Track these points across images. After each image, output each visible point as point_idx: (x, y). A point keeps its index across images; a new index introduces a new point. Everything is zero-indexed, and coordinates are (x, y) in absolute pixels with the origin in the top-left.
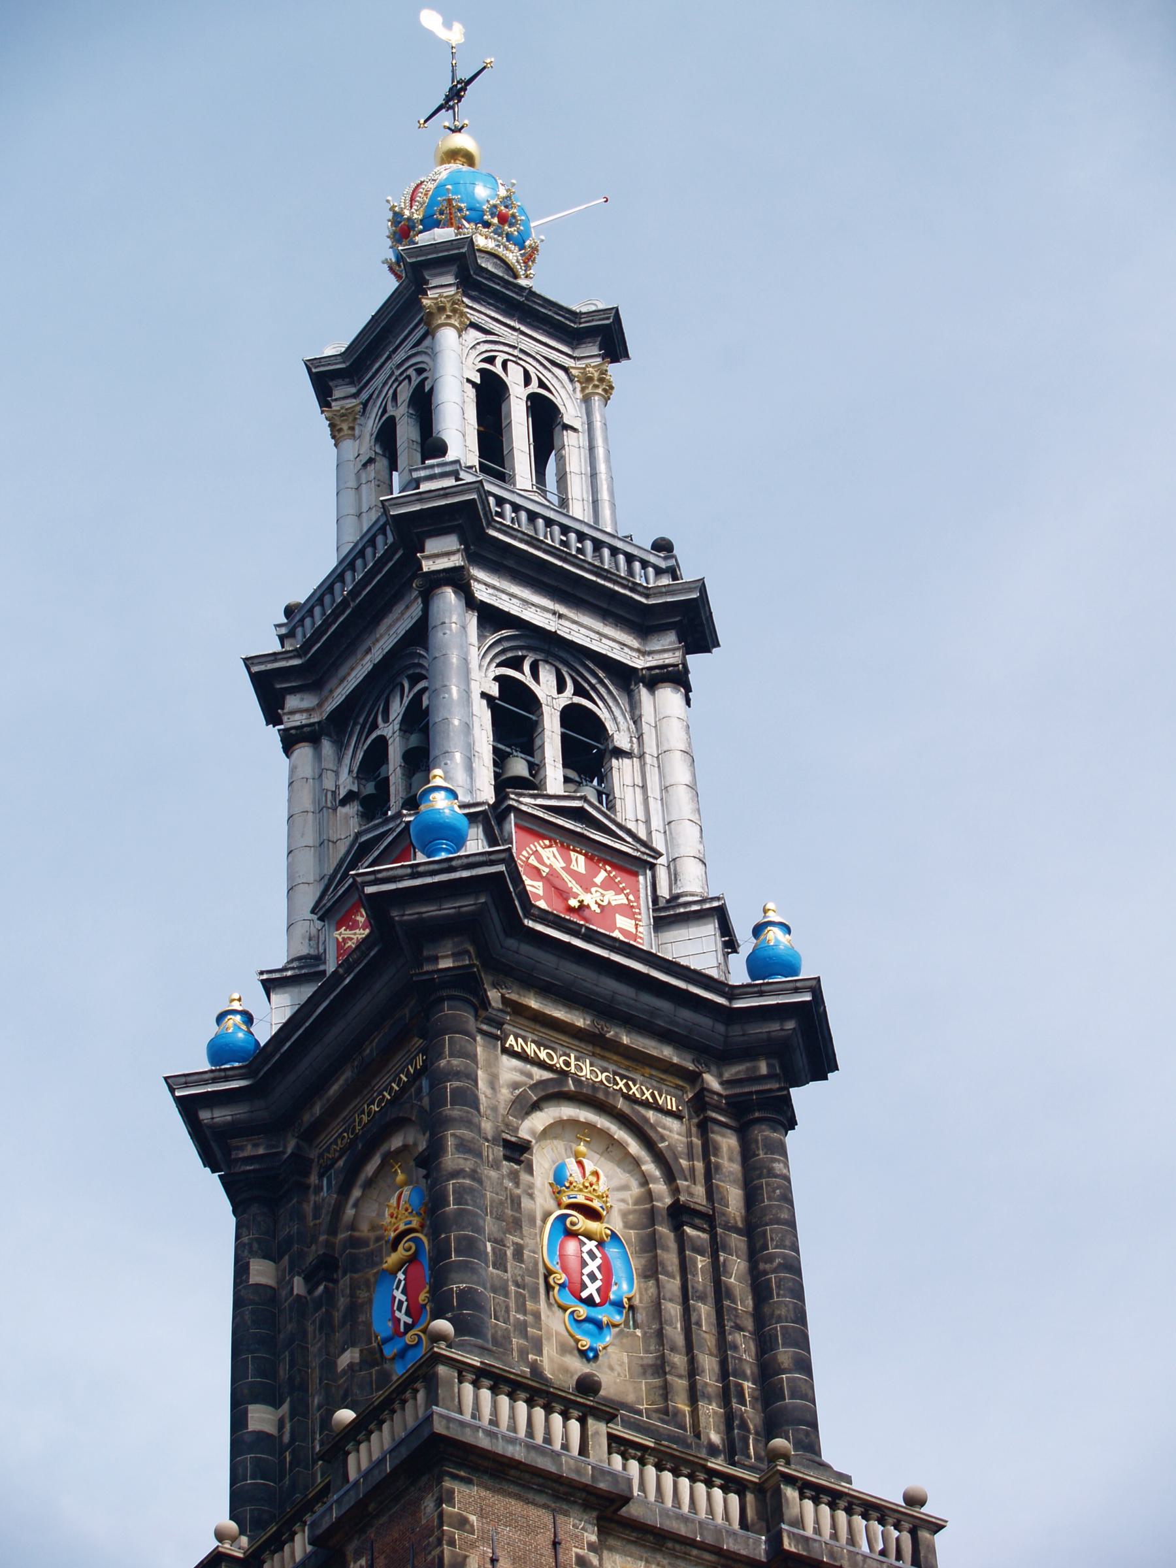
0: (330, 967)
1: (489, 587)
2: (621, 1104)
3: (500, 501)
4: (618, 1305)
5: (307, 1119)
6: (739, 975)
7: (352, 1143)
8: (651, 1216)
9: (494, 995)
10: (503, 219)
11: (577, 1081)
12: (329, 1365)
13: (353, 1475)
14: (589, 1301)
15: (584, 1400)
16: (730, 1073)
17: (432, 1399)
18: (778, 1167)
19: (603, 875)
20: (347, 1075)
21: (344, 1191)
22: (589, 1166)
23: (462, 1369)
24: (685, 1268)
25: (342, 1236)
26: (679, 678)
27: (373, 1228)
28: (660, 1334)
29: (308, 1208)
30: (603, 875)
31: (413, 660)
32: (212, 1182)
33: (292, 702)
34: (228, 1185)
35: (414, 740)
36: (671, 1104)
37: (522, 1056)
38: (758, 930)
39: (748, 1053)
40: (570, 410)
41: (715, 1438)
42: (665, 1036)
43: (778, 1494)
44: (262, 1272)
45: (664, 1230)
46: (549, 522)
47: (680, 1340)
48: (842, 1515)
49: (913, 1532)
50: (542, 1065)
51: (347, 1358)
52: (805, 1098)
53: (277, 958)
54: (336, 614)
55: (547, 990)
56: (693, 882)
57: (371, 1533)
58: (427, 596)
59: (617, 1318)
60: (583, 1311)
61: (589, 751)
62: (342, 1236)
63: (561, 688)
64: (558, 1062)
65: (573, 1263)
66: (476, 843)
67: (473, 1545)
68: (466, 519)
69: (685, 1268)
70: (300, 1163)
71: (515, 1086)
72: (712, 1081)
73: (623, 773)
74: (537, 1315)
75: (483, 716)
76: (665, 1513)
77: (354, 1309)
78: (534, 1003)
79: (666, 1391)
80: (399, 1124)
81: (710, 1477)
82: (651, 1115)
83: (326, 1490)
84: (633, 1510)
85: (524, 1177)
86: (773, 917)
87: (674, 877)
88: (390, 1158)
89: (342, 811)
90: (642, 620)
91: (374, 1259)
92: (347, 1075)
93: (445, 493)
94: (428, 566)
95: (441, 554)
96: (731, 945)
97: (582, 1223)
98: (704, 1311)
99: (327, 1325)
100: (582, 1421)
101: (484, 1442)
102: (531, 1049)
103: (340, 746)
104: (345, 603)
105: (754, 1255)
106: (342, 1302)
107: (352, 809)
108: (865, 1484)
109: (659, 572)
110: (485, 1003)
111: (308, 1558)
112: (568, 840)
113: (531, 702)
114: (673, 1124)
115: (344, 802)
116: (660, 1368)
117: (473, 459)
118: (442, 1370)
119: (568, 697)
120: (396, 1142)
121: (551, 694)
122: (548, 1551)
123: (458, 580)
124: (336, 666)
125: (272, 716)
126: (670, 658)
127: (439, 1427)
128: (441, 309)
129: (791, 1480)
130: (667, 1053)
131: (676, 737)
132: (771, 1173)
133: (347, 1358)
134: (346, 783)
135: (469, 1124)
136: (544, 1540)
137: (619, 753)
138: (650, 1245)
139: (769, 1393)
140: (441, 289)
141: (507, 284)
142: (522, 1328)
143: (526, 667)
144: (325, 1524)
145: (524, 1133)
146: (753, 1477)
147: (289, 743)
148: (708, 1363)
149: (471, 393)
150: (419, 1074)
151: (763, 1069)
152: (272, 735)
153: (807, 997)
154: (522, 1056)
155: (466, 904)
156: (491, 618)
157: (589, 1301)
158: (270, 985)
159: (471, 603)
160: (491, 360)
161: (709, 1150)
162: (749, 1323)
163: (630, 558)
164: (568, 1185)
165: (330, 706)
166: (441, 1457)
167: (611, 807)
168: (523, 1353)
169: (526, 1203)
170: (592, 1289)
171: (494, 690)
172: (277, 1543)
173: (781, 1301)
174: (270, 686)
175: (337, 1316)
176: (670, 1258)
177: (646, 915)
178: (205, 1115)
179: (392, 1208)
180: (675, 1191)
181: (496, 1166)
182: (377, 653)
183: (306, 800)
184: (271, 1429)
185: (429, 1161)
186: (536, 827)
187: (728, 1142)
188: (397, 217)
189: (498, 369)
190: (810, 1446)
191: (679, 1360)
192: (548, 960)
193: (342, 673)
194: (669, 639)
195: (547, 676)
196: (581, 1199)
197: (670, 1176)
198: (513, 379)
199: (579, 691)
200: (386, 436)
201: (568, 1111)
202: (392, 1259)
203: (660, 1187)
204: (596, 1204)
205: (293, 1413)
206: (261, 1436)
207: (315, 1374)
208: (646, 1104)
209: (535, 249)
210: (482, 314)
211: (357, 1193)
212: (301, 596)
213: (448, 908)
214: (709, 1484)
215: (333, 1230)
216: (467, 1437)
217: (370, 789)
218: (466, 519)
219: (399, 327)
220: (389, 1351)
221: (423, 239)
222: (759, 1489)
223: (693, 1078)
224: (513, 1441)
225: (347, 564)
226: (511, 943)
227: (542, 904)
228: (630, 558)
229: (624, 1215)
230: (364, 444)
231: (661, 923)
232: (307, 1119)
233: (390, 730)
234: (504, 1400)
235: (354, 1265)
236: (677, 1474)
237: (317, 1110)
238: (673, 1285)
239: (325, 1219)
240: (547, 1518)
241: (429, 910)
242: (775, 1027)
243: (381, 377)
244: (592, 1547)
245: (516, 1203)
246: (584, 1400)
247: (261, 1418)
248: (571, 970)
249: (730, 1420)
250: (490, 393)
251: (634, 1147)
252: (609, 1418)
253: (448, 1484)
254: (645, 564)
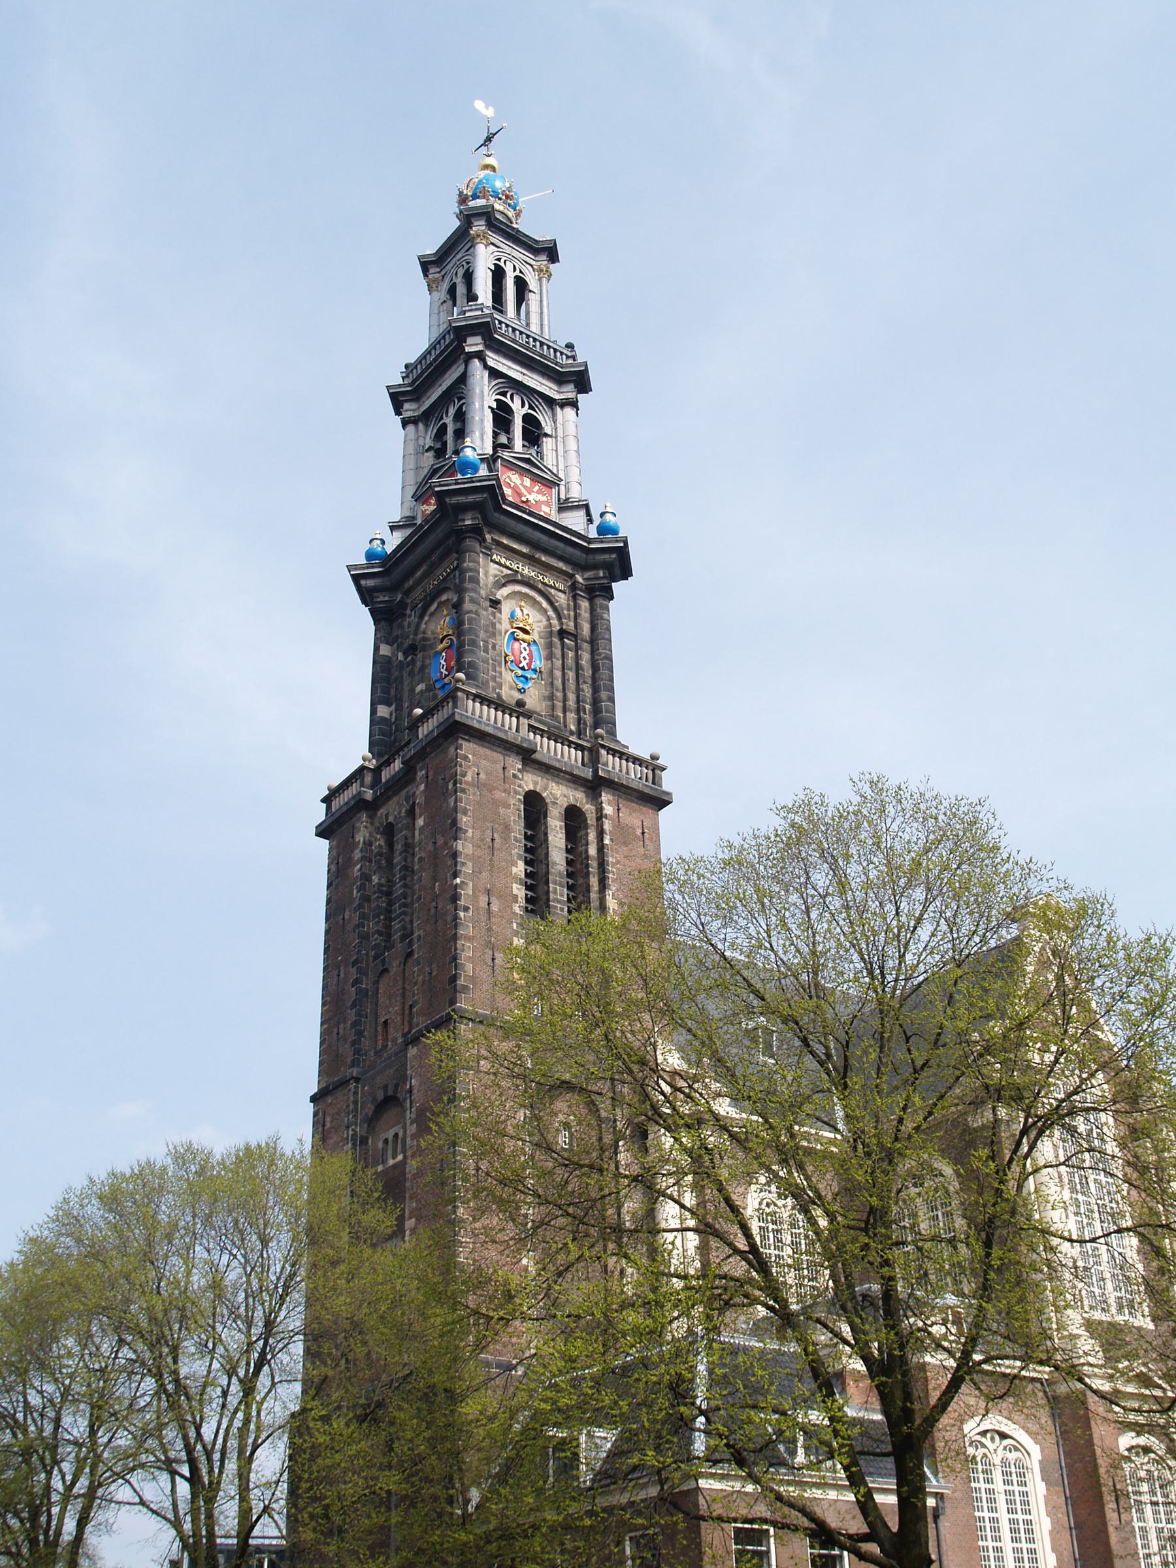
0: (419, 522)
1: (494, 360)
2: (540, 586)
3: (500, 322)
4: (535, 670)
5: (407, 585)
6: (593, 534)
7: (426, 597)
8: (551, 634)
9: (488, 537)
10: (507, 197)
11: (522, 575)
12: (412, 690)
13: (420, 736)
14: (523, 669)
15: (519, 710)
16: (588, 574)
17: (455, 706)
18: (605, 616)
19: (537, 488)
20: (424, 568)
21: (421, 617)
22: (526, 612)
23: (468, 694)
24: (563, 656)
25: (420, 636)
26: (574, 404)
27: (433, 633)
28: (552, 684)
29: (406, 624)
30: (537, 488)
31: (459, 390)
32: (366, 610)
33: (406, 406)
34: (372, 612)
35: (459, 425)
36: (562, 587)
37: (499, 564)
38: (602, 515)
39: (595, 567)
40: (533, 283)
41: (573, 728)
42: (560, 558)
43: (598, 752)
44: (385, 650)
45: (556, 640)
46: (521, 333)
47: (560, 687)
48: (624, 762)
49: (653, 771)
50: (507, 568)
51: (420, 687)
52: (617, 587)
53: (396, 516)
54: (427, 369)
56: (575, 493)
57: (427, 760)
58: (467, 363)
59: (534, 676)
60: (520, 672)
61: (533, 433)
62: (420, 636)
63: (523, 406)
64: (515, 567)
65: (517, 652)
66: (483, 471)
67: (470, 767)
68: (485, 330)
69: (563, 656)
70: (403, 605)
71: (496, 576)
72: (579, 578)
73: (548, 444)
74: (501, 673)
75: (489, 416)
76: (550, 758)
77: (423, 668)
78: (505, 541)
79: (553, 707)
80: (446, 589)
81: (570, 744)
82: (552, 591)
83: (409, 742)
84: (536, 756)
85: (498, 615)
86: (608, 509)
87: (567, 490)
88: (441, 604)
89: (426, 454)
90: (559, 378)
91: (432, 646)
92: (424, 568)
93: (476, 317)
94: (467, 349)
95: (474, 344)
96: (590, 521)
97: (521, 635)
98: (571, 675)
99: (411, 674)
100: (518, 718)
101: (476, 725)
102: (503, 561)
103: (427, 426)
104: (431, 364)
105: (593, 652)
106: (419, 664)
107: (431, 454)
108: (634, 750)
109: (568, 357)
110: (484, 540)
111: (401, 769)
112: (523, 472)
113: (510, 411)
114: (562, 596)
115: (427, 451)
116: (551, 698)
117: (490, 303)
118: (459, 694)
119: (526, 410)
120: (444, 598)
121: (519, 410)
122: (501, 771)
123: (480, 356)
124: (426, 391)
125: (398, 412)
126: (570, 395)
127: (457, 718)
128: (479, 236)
129: (603, 747)
130: (561, 565)
131: (571, 430)
132: (602, 618)
133: (420, 687)
134: (429, 442)
135: (475, 591)
136: (499, 766)
137: (546, 435)
138: (550, 646)
139: (596, 710)
140: (479, 226)
141: (508, 226)
142: (494, 678)
143: (508, 395)
144: (408, 756)
145: (498, 597)
146: (588, 745)
147: (405, 424)
148: (572, 697)
149: (490, 274)
150: (455, 569)
151: (601, 574)
152: (398, 420)
153: (622, 545)
154: (499, 564)
155: (478, 497)
156: (494, 373)
157: (523, 669)
158: (392, 528)
159: (486, 366)
160: (499, 260)
161: (576, 607)
162: (590, 681)
163: (555, 350)
164: (514, 619)
165: (423, 409)
166: (456, 730)
167: (542, 458)
168: (494, 689)
169: (498, 625)
170: (524, 663)
171: (494, 405)
172: (388, 763)
173: (603, 672)
174: (397, 399)
175: (416, 670)
177: (555, 506)
178: (363, 582)
179: (439, 625)
180: (561, 624)
181: (486, 609)
182: (444, 387)
183: (411, 450)
184: (387, 716)
185: (457, 606)
186: (509, 465)
187: (584, 604)
188: (461, 193)
189: (502, 264)
190: (612, 733)
191: (559, 695)
192: (512, 523)
193: (428, 394)
194: (571, 387)
195: (517, 400)
196: (521, 625)
197: (559, 617)
198: (508, 269)
199: (531, 407)
200: (452, 291)
201: (518, 588)
202: (441, 647)
203: (555, 622)
204: (528, 628)
205: (396, 710)
206: (383, 719)
207: (406, 694)
208: (551, 586)
209: (521, 211)
210: (496, 238)
211: (426, 618)
212: (412, 360)
213: (470, 499)
214: (569, 747)
215: (416, 634)
216: (469, 722)
217: (439, 445)
218: (485, 330)
219: (460, 242)
220: (438, 685)
221: (472, 204)
222: (590, 750)
223: (572, 576)
224: (488, 725)
225: (433, 347)
226: (496, 515)
227: (510, 499)
228: (555, 350)
229: (539, 633)
230: (442, 294)
231: (561, 510)
232: (407, 585)
233: (448, 420)
234: (485, 708)
235: (424, 649)
236: (556, 742)
237: (411, 582)
239: (412, 628)
240: (501, 757)
241: (462, 499)
242: (606, 556)
243: (451, 265)
244: (519, 770)
245: (494, 625)
246: (519, 710)
247: (383, 711)
248: (521, 528)
249: (579, 720)
250: (498, 274)
251: (545, 604)
252: (529, 717)
253: (460, 741)
254: (562, 353)
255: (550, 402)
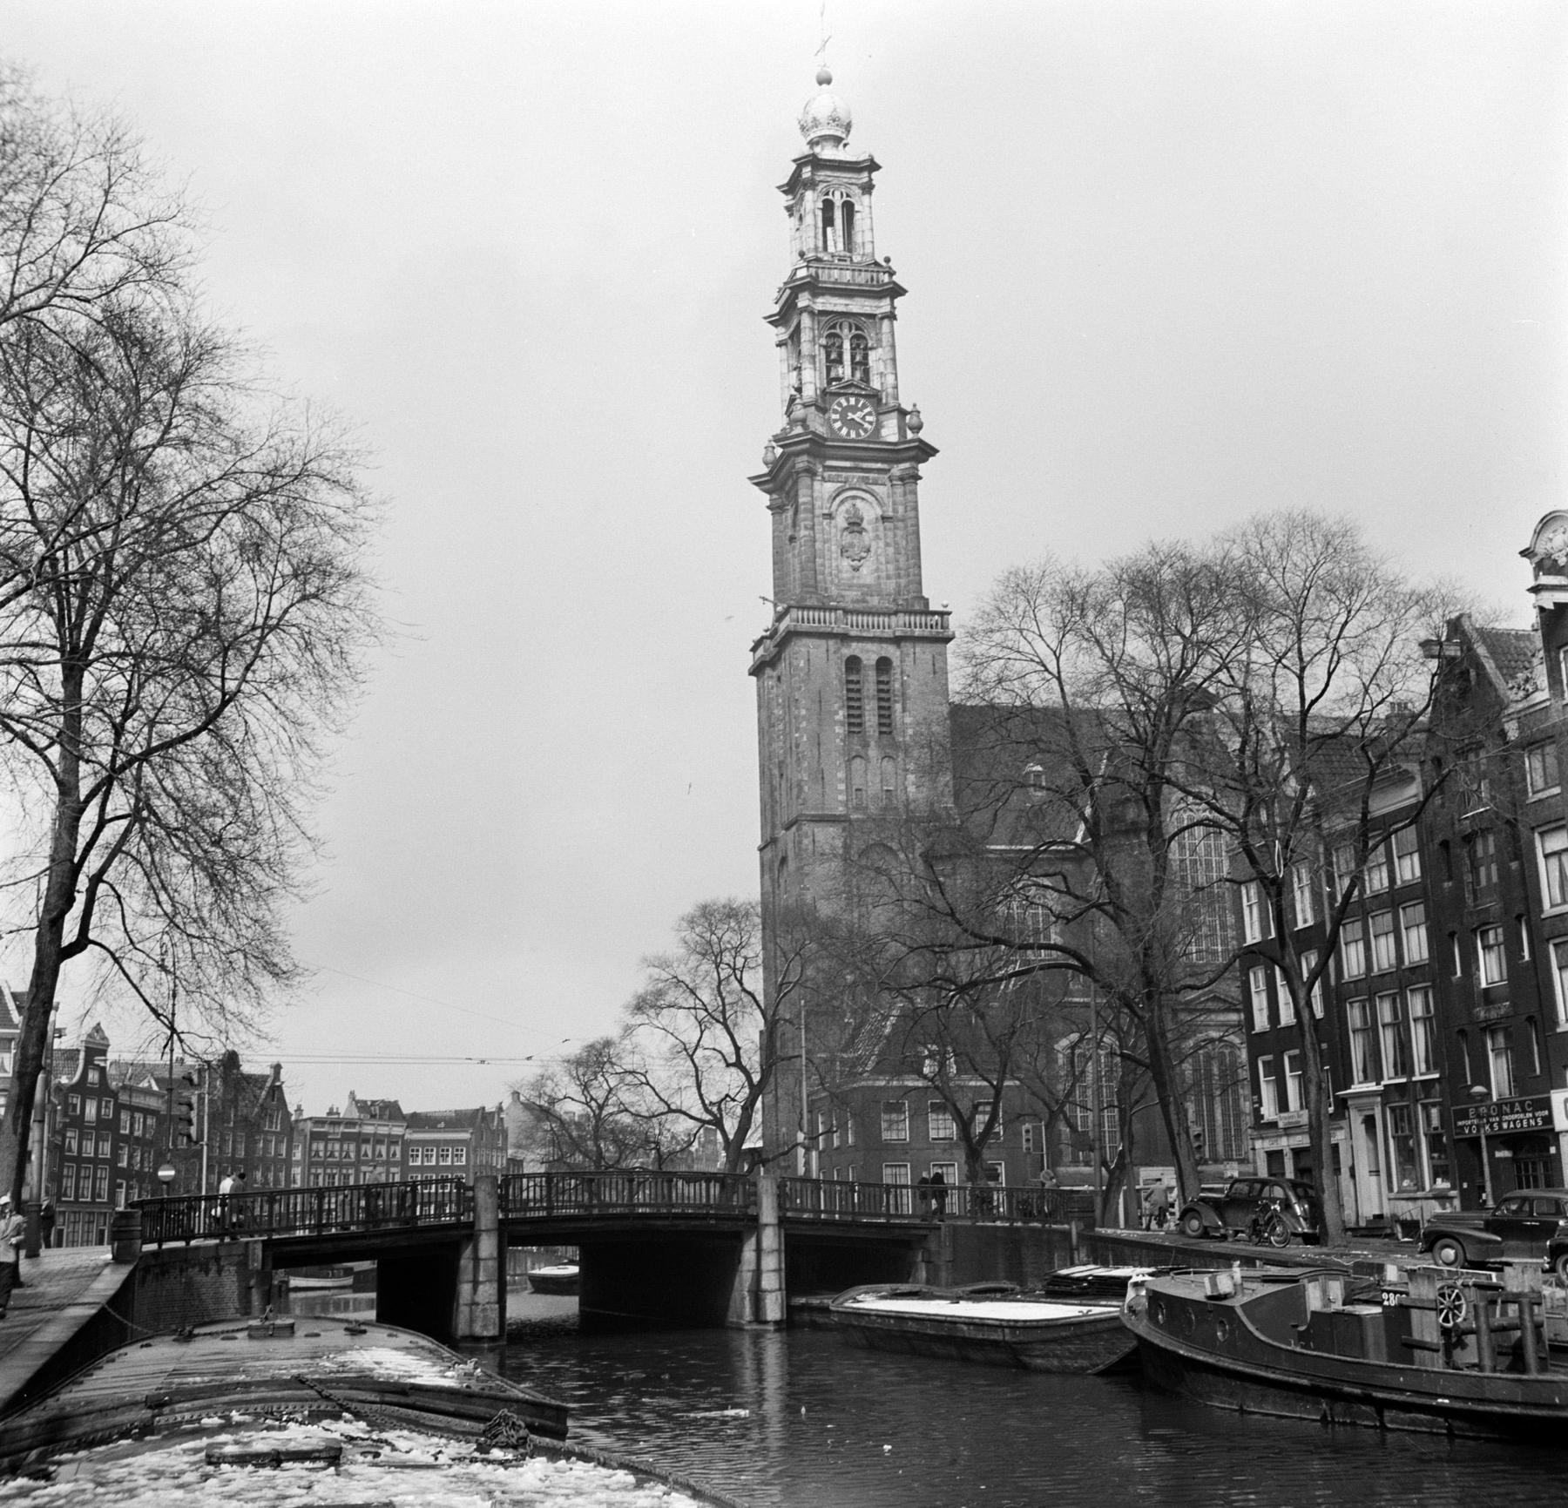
26: (892, 316)
42: (877, 461)
55: (836, 459)
73: (872, 356)
116: (877, 570)
130: (879, 465)
176: (881, 534)
192: (833, 452)
199: (858, 328)
238: (882, 544)
250: (828, 206)
255: (872, 316)
